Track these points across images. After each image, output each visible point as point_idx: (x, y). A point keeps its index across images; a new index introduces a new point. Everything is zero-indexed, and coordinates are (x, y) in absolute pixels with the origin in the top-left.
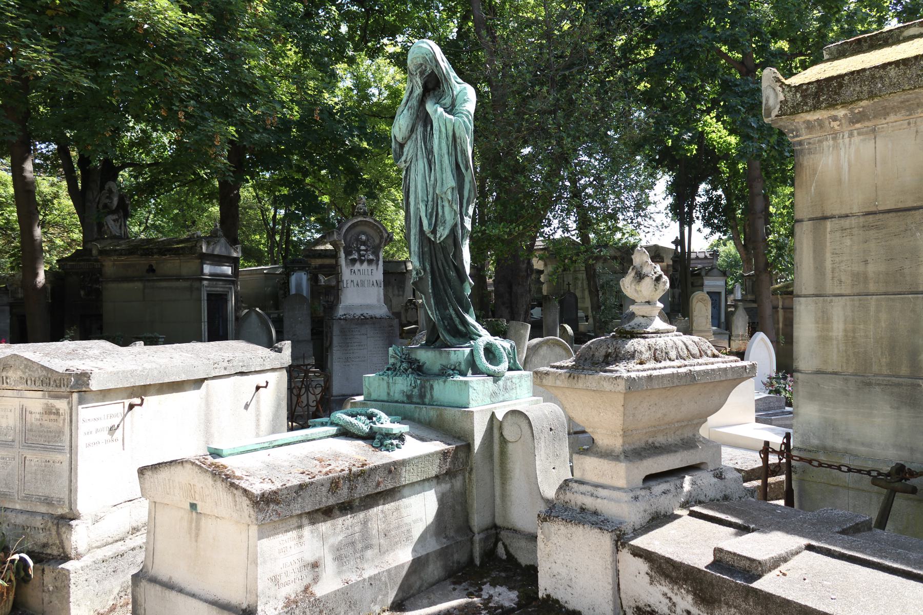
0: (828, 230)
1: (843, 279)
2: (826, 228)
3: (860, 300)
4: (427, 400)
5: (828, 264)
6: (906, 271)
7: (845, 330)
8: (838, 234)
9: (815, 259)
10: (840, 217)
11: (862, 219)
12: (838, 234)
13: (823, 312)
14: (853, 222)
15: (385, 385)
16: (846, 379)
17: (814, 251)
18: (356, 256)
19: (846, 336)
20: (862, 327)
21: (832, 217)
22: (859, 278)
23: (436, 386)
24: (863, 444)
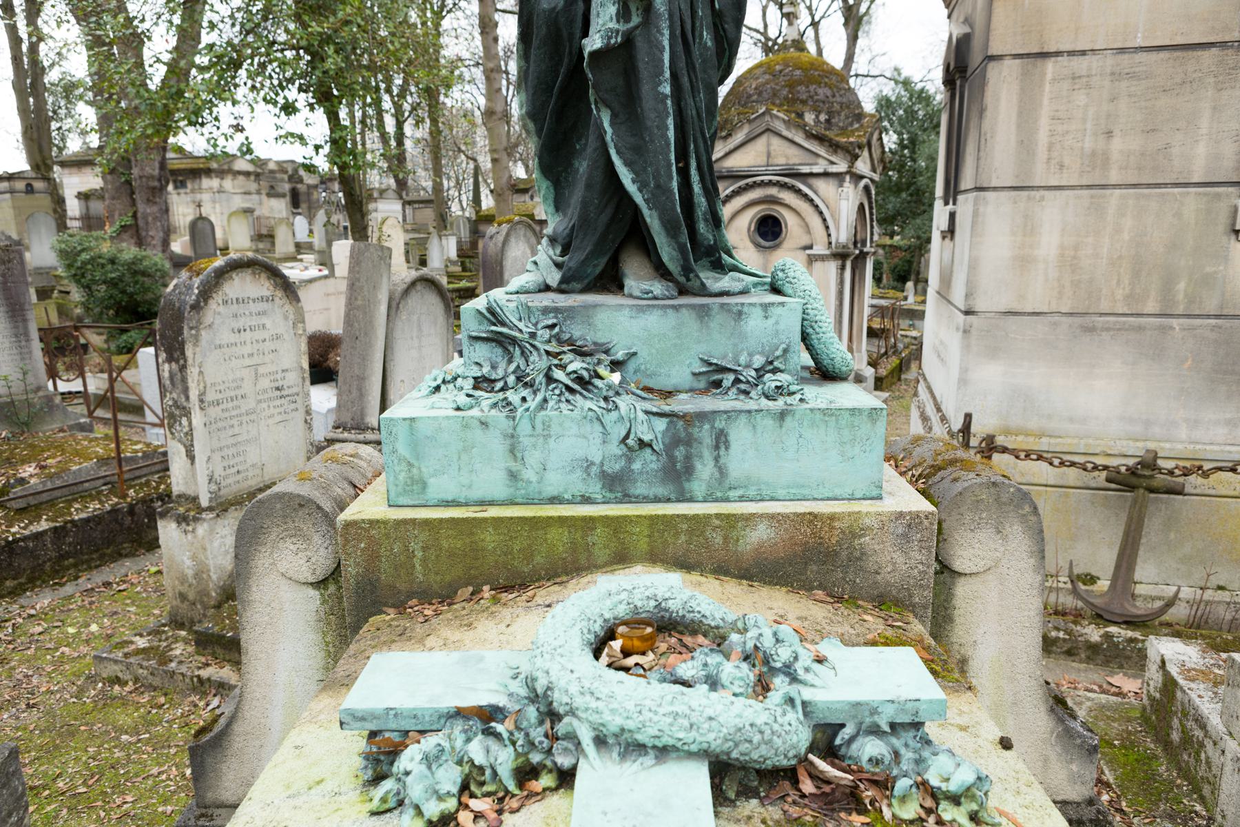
0: (1049, 76)
1: (1067, 161)
2: (1043, 74)
3: (1092, 197)
4: (697, 487)
5: (1043, 137)
6: (1175, 151)
7: (1062, 247)
8: (1066, 85)
9: (1019, 126)
10: (1071, 53)
11: (1110, 61)
12: (1066, 85)
13: (1026, 217)
14: (1095, 65)
16: (1055, 324)
17: (1020, 114)
19: (1062, 255)
20: (1090, 240)
21: (1058, 54)
22: (1100, 159)
23: (739, 434)
24: (1071, 420)
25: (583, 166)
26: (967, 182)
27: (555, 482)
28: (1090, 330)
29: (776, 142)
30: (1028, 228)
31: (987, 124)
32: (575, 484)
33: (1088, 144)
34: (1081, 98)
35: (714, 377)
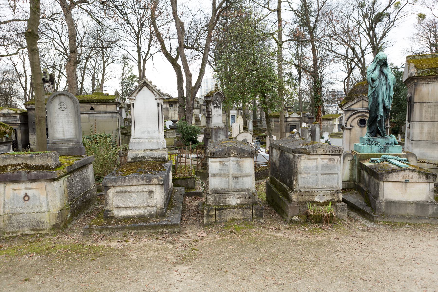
5: (424, 114)
11: (434, 104)
15: (370, 148)
18: (215, 105)
23: (390, 148)
25: (373, 127)
26: (411, 120)
27: (375, 151)
28: (434, 143)
29: (365, 102)
30: (422, 128)
31: (414, 113)
32: (376, 152)
33: (431, 115)
34: (430, 109)
35: (387, 144)
